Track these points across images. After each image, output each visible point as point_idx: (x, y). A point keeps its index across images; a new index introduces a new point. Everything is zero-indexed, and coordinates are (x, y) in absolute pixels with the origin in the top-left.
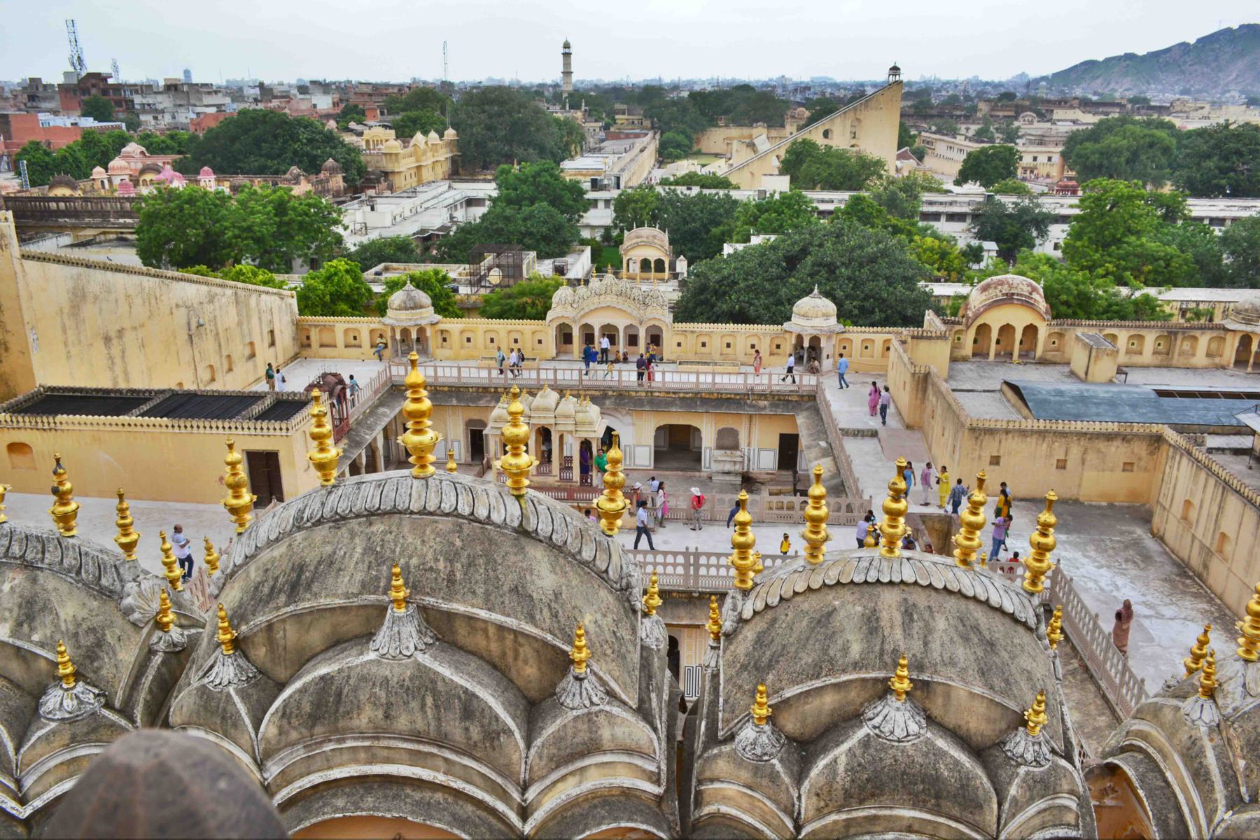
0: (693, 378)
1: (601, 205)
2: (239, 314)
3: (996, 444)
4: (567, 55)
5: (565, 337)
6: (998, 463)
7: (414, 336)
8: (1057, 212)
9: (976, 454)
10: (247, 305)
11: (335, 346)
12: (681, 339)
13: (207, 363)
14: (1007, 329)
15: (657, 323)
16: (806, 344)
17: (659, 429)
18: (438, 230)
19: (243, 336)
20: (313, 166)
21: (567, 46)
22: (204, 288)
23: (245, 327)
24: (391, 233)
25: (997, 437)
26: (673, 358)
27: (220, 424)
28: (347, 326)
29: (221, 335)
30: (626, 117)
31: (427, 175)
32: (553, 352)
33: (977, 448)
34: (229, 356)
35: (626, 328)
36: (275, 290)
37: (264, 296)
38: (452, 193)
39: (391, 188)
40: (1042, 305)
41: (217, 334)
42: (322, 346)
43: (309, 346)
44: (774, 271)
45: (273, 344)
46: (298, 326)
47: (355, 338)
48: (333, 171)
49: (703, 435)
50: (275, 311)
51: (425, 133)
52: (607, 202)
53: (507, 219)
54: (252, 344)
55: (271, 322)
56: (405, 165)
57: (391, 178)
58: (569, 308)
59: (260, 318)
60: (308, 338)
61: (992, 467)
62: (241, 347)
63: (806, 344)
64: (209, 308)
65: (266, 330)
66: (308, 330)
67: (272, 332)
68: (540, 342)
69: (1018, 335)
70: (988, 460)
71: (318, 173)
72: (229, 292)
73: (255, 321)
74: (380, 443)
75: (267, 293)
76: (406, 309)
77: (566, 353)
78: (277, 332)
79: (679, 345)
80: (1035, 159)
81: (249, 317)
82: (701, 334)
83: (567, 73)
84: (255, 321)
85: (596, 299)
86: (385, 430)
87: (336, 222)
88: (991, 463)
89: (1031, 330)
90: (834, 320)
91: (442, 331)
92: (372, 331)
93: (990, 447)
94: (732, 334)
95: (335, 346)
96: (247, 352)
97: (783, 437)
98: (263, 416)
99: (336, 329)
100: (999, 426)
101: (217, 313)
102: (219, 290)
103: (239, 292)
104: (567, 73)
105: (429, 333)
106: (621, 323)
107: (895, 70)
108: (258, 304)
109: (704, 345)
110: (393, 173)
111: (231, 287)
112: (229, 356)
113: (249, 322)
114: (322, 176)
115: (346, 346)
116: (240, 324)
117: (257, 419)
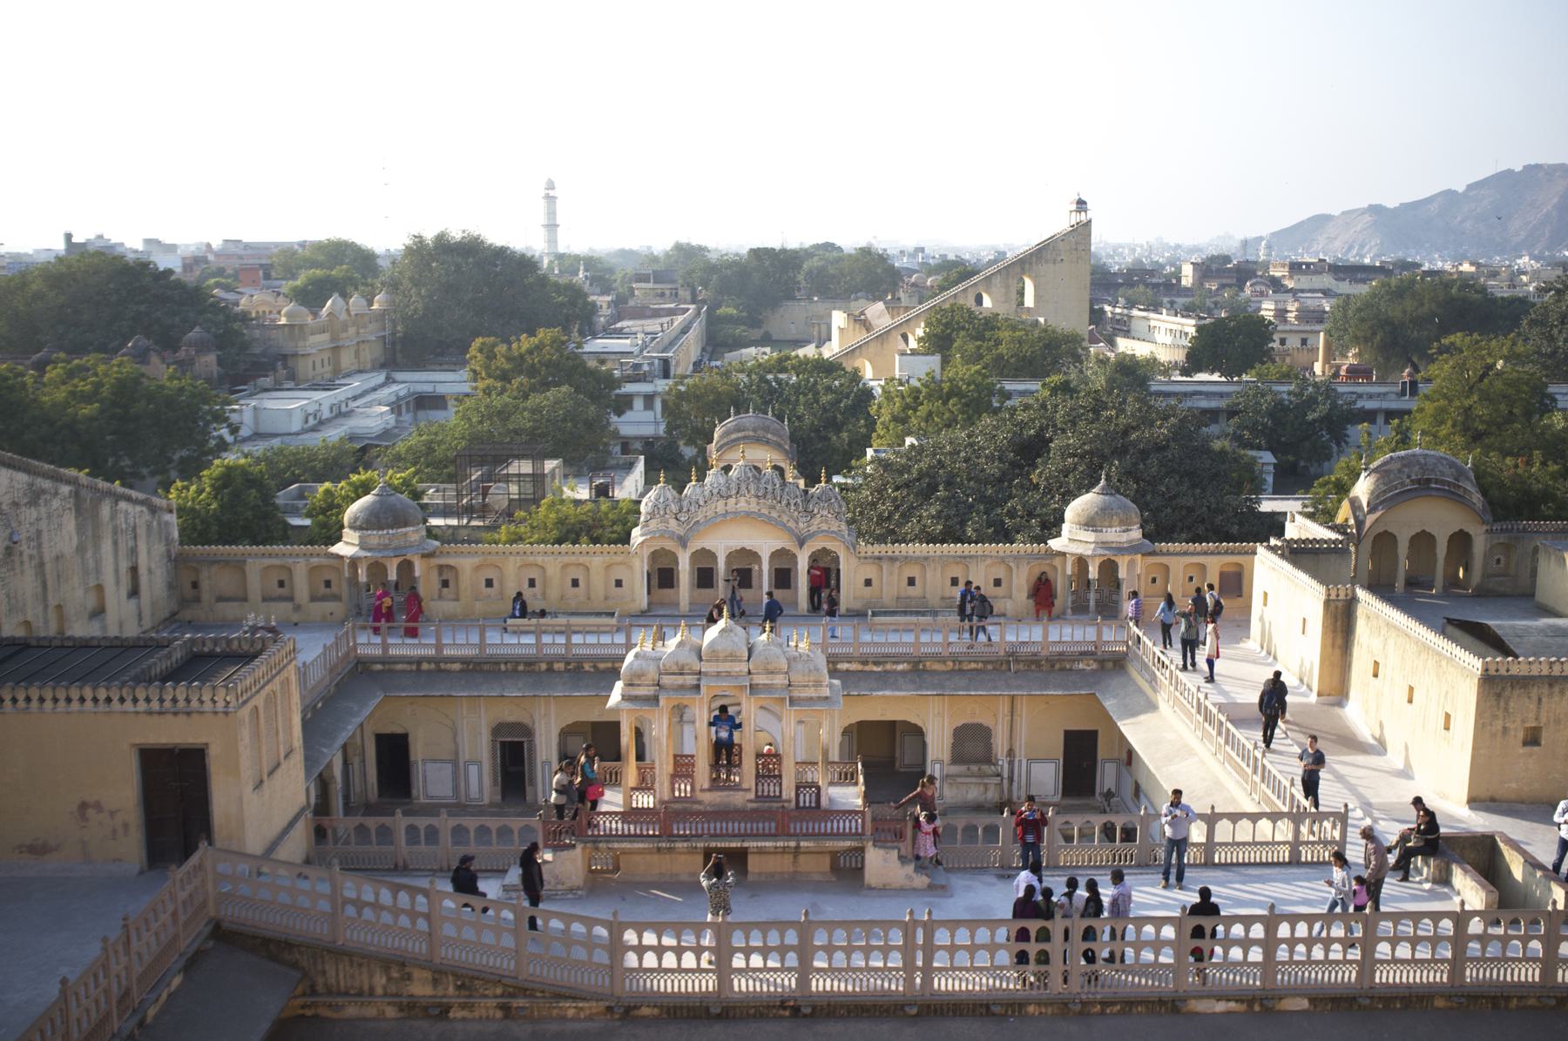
0: (909, 638)
1: (638, 404)
2: (80, 529)
3: (1533, 706)
4: (550, 199)
5: (664, 577)
7: (393, 576)
8: (1359, 404)
9: (1499, 724)
10: (96, 515)
11: (245, 599)
12: (870, 571)
13: (21, 618)
14: (1423, 541)
15: (830, 545)
16: (1093, 572)
17: (847, 732)
18: (379, 437)
19: (86, 573)
20: (168, 342)
21: (551, 185)
22: (22, 477)
23: (89, 554)
24: (295, 444)
25: (1534, 692)
26: (857, 605)
27: (88, 692)
28: (268, 562)
29: (48, 567)
30: (650, 285)
31: (347, 360)
32: (642, 599)
33: (1500, 713)
34: (59, 607)
36: (141, 496)
37: (123, 505)
38: (394, 388)
39: (292, 376)
40: (1477, 498)
41: (41, 565)
42: (220, 599)
43: (198, 600)
44: (993, 469)
45: (134, 592)
46: (177, 562)
47: (281, 584)
48: (202, 347)
49: (929, 739)
50: (141, 531)
51: (345, 296)
52: (649, 399)
53: (503, 414)
54: (100, 588)
55: (134, 551)
56: (317, 342)
57: (290, 363)
58: (673, 522)
59: (115, 543)
60: (195, 585)
61: (1528, 749)
62: (80, 593)
63: (1093, 572)
64: (29, 514)
65: (124, 565)
66: (197, 571)
67: (134, 570)
68: (619, 583)
70: (1521, 735)
71: (176, 349)
72: (65, 489)
73: (107, 546)
74: (337, 771)
75: (129, 499)
76: (381, 528)
77: (662, 604)
78: (143, 571)
79: (868, 583)
81: (97, 539)
82: (907, 559)
83: (552, 227)
84: (107, 546)
85: (721, 503)
86: (345, 747)
87: (220, 418)
88: (1525, 743)
89: (1461, 541)
90: (1136, 534)
91: (441, 568)
92: (313, 570)
93: (1524, 711)
94: (963, 559)
95: (245, 599)
96: (91, 602)
97: (1069, 735)
98: (174, 675)
99: (247, 568)
100: (1535, 672)
101: (43, 525)
102: (47, 484)
103: (83, 492)
104: (552, 227)
105: (418, 572)
106: (765, 543)
107: (1081, 204)
108: (113, 516)
109: (911, 582)
110: (295, 355)
111: (68, 482)
112: (59, 607)
113: (97, 547)
114: (182, 354)
115: (264, 600)
116: (81, 549)
117: (164, 680)
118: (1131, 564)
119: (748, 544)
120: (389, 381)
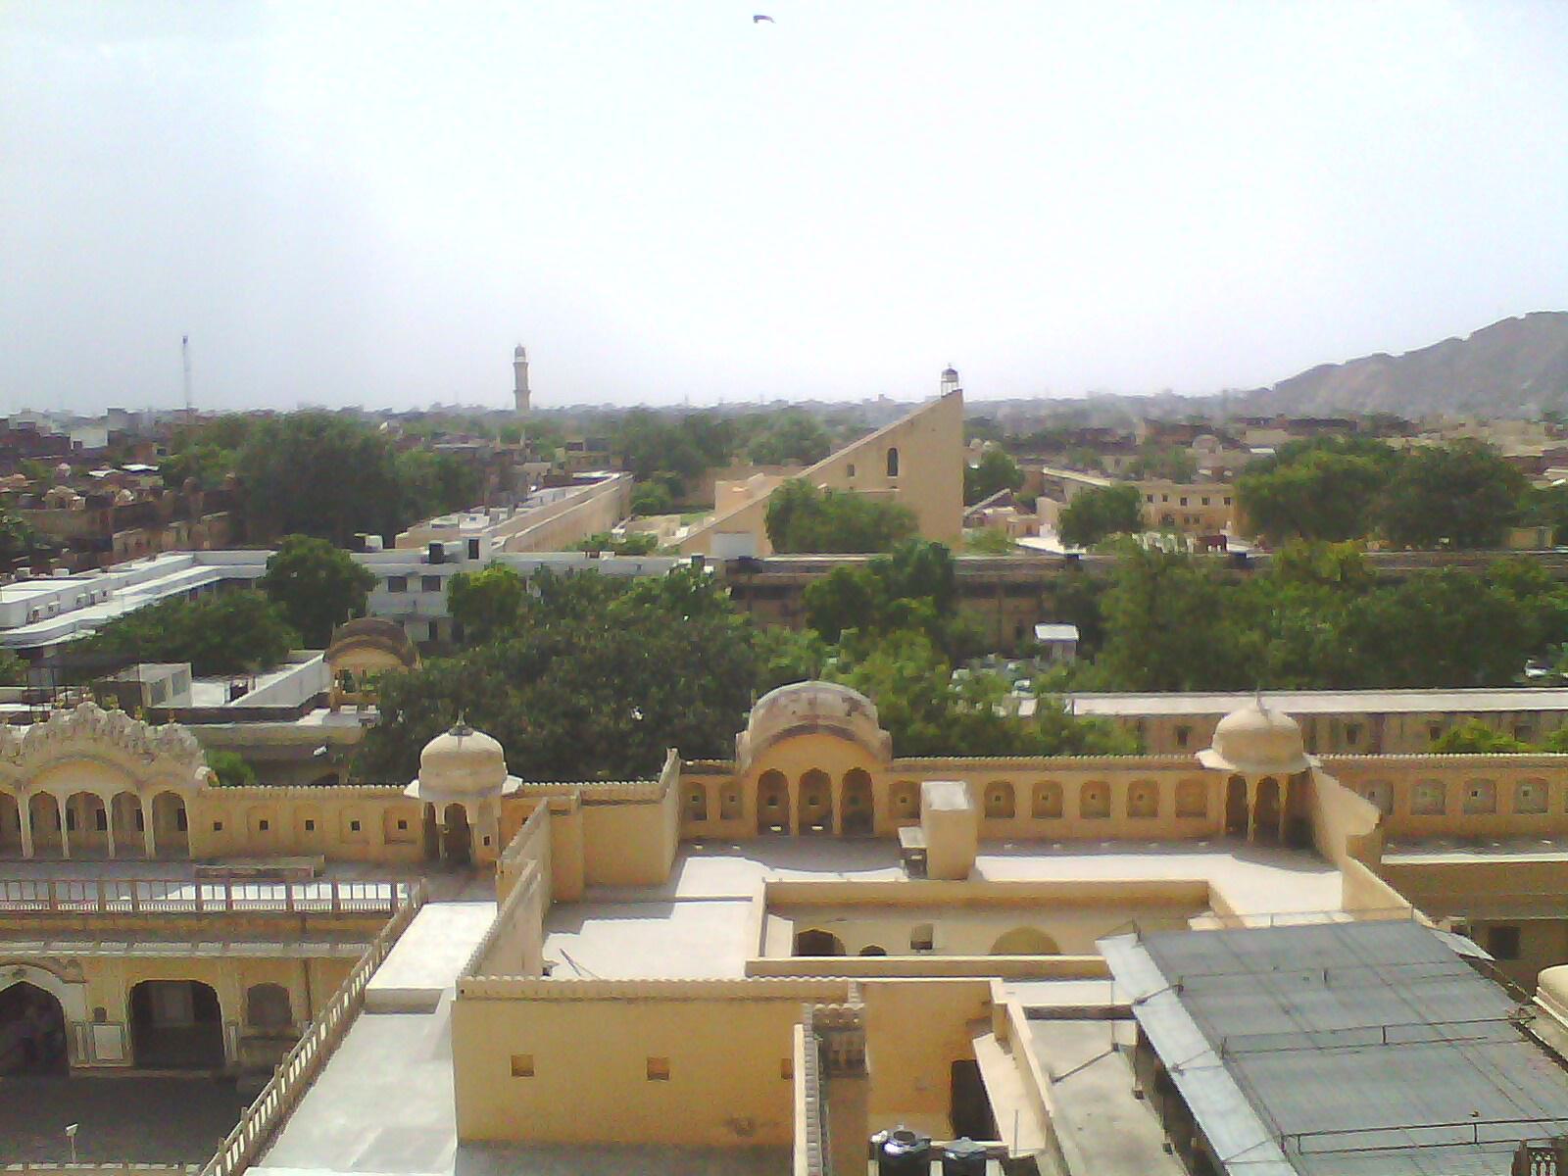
6: (516, 1073)
14: (814, 780)
21: (520, 352)
30: (583, 454)
35: (117, 800)
69: (837, 794)
79: (218, 826)
80: (1184, 501)
83: (522, 391)
104: (522, 391)
106: (106, 789)
107: (951, 374)
118: (484, 809)
119: (93, 788)
120: (196, 562)
